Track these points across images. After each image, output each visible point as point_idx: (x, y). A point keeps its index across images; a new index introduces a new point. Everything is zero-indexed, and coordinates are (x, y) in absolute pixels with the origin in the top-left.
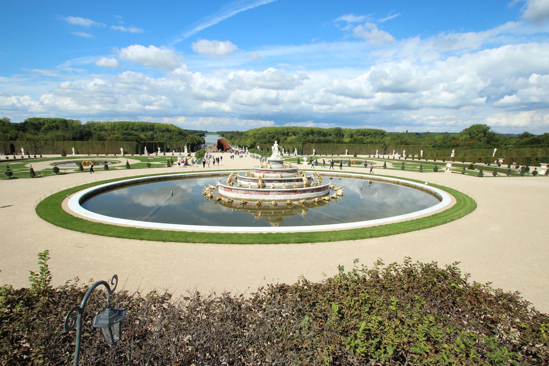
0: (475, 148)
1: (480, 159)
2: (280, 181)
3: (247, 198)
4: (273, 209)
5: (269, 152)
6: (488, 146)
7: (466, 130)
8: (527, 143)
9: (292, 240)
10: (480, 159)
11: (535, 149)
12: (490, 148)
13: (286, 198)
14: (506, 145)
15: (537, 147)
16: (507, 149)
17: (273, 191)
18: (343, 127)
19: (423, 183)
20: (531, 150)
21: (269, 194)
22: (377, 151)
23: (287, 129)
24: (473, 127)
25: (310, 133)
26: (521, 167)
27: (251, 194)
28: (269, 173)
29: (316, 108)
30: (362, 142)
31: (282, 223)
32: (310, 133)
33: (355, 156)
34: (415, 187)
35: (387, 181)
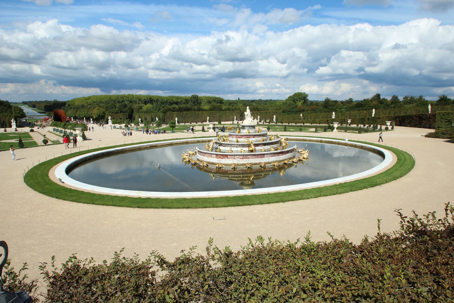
0: (318, 112)
1: (328, 121)
2: (265, 144)
3: (245, 163)
4: (232, 174)
5: (242, 117)
6: (326, 109)
7: (290, 97)
8: (355, 107)
9: (257, 201)
10: (328, 121)
11: (361, 111)
12: (329, 112)
13: (277, 160)
14: (340, 109)
15: (363, 110)
16: (341, 112)
17: (267, 154)
18: (201, 95)
19: (345, 140)
20: (359, 112)
21: (264, 157)
22: (235, 117)
23: (122, 97)
24: (295, 94)
25: (148, 102)
26: (372, 126)
27: (248, 158)
28: (249, 137)
29: (153, 75)
30: (220, 110)
31: (252, 185)
32: (148, 102)
33: (220, 123)
34: (339, 144)
35: (311, 141)
